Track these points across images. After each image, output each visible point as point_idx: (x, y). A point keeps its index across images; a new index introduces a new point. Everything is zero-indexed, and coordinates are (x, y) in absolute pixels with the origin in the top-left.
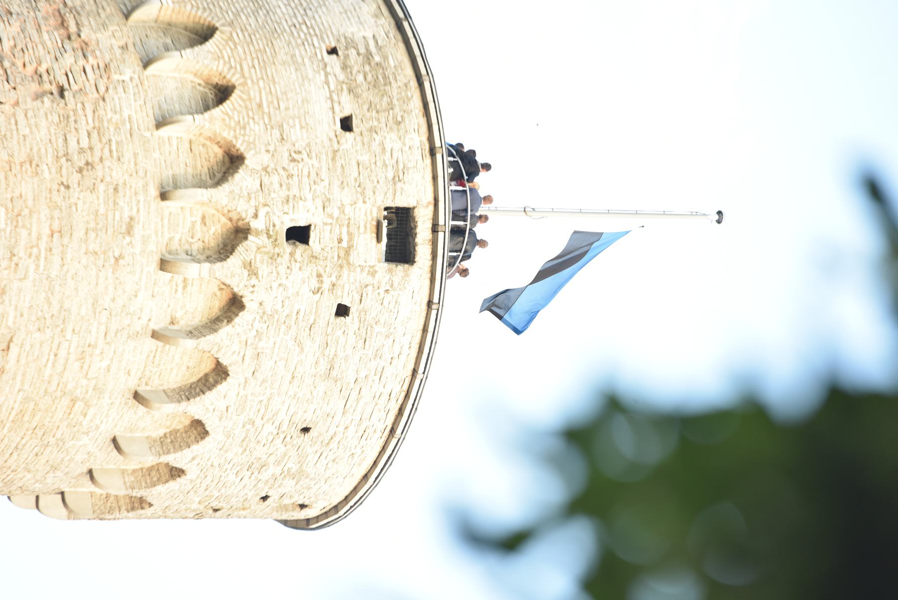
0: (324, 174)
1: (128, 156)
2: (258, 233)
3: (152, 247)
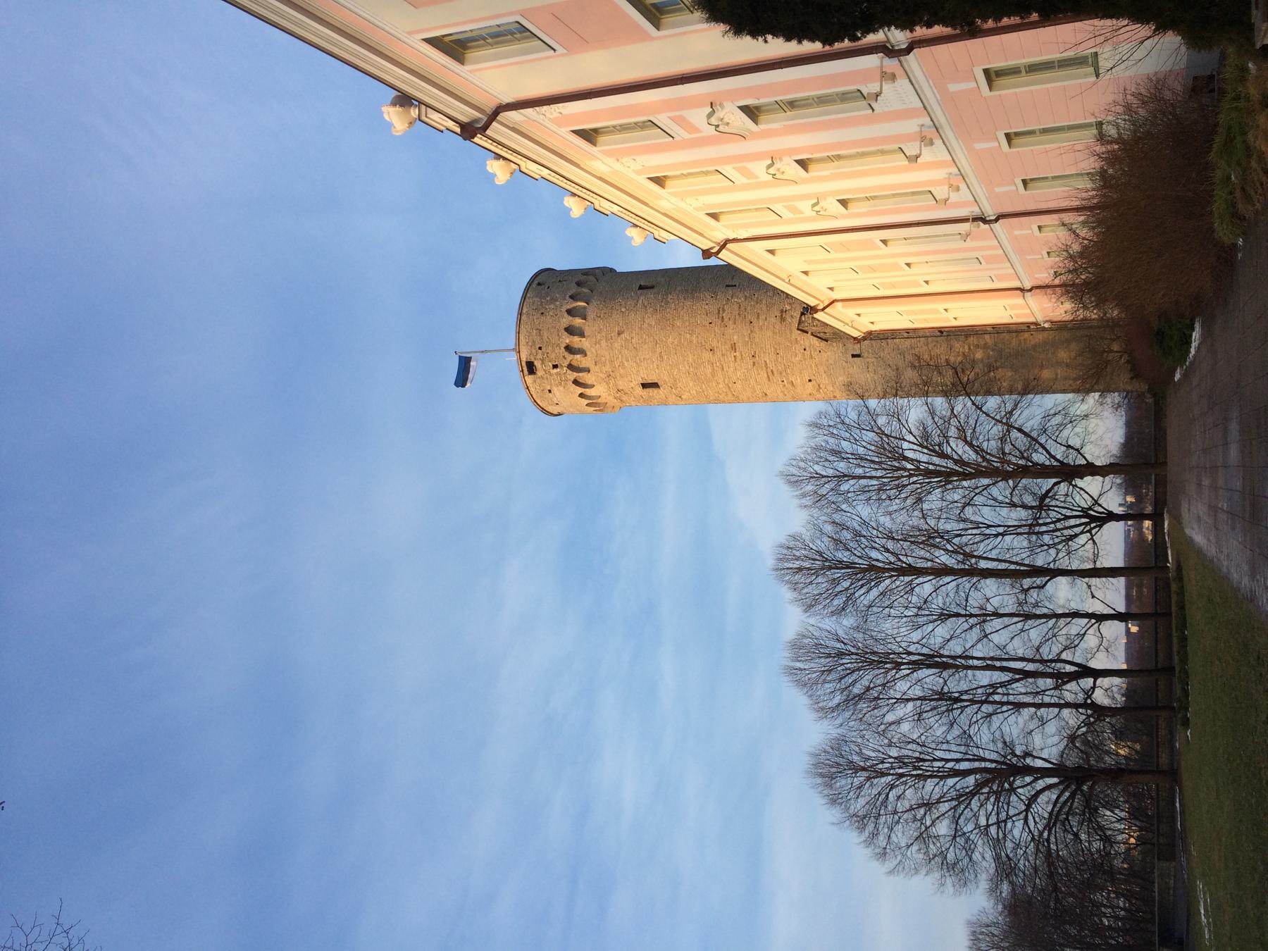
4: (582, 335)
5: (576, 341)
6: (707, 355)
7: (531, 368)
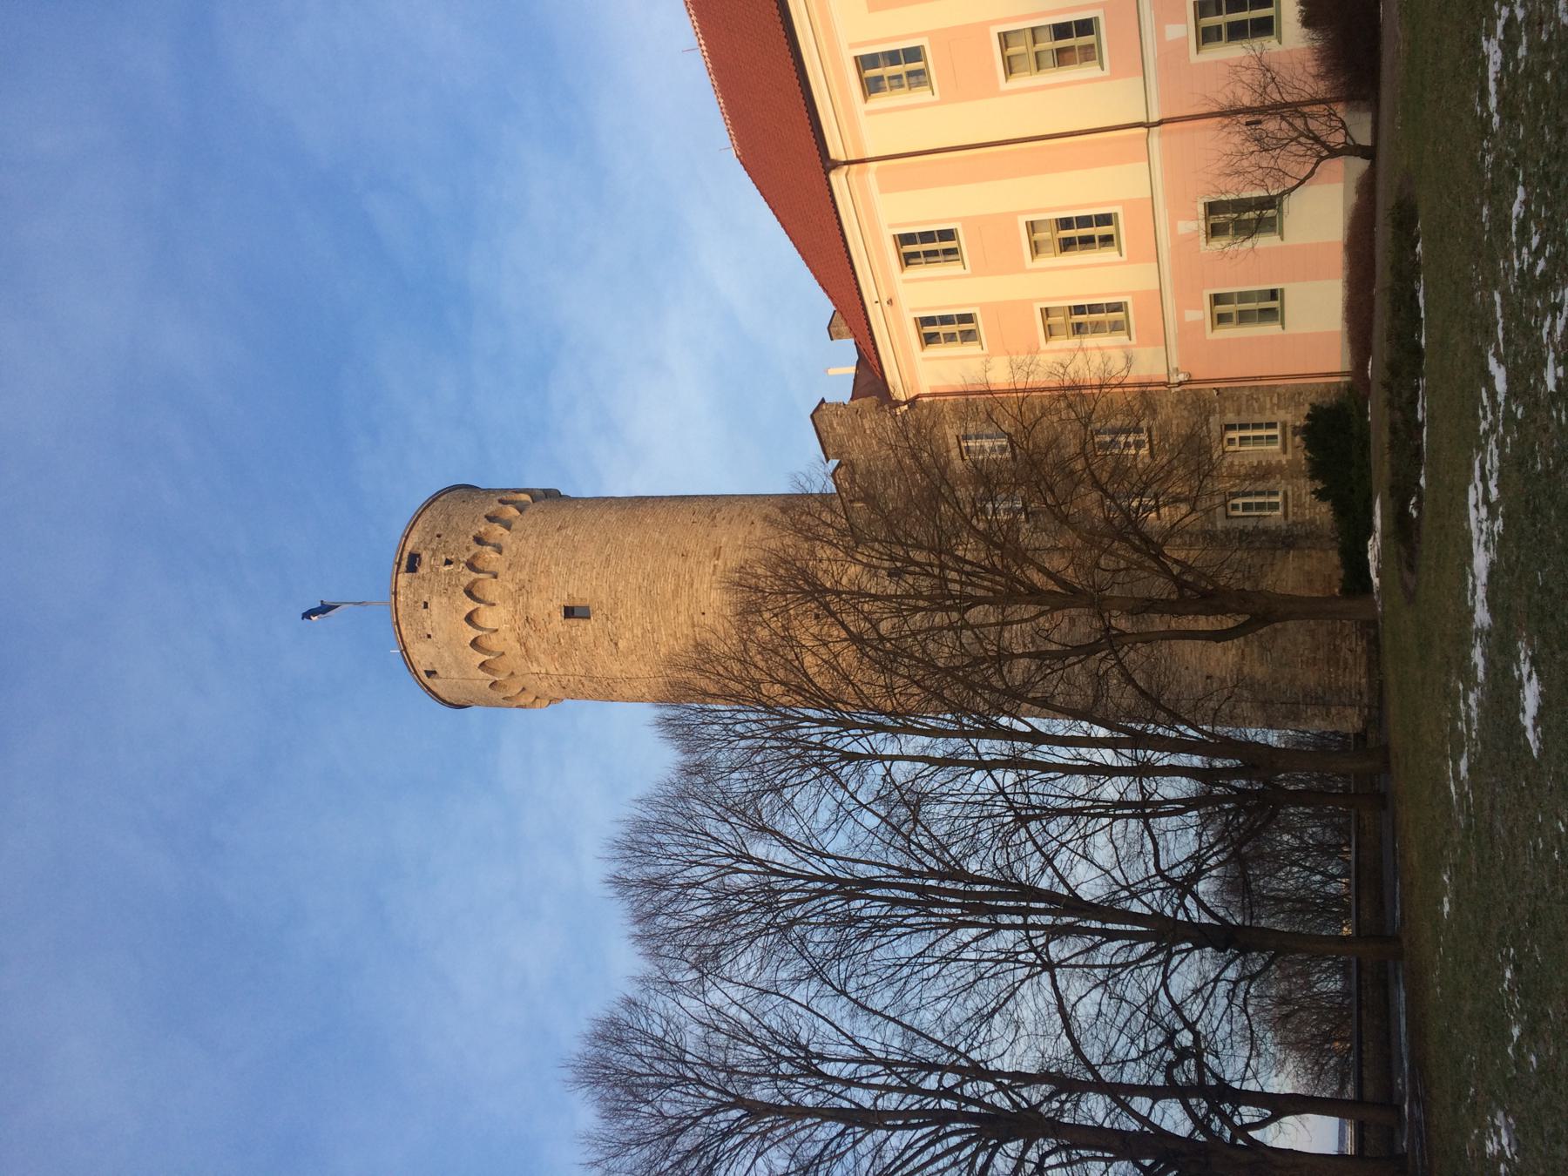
4: (508, 527)
6: (674, 562)
7: (413, 563)
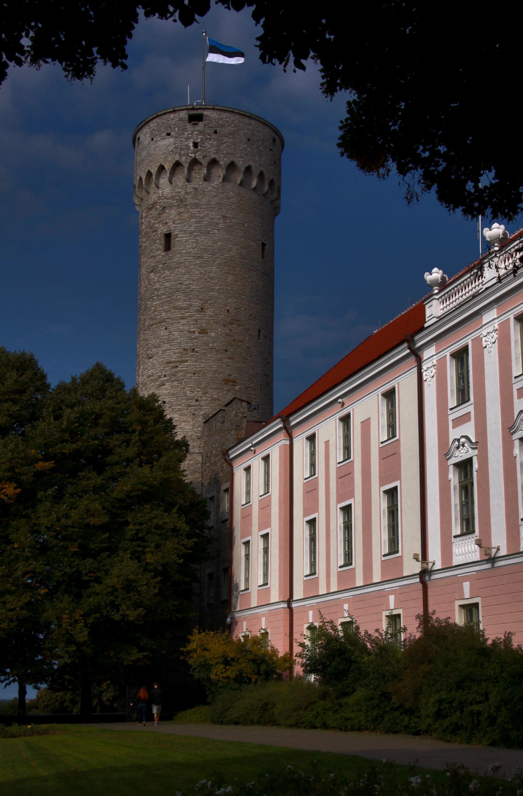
0: (181, 139)
1: (179, 190)
2: (195, 156)
3: (201, 183)
5: (219, 173)
6: (197, 304)
